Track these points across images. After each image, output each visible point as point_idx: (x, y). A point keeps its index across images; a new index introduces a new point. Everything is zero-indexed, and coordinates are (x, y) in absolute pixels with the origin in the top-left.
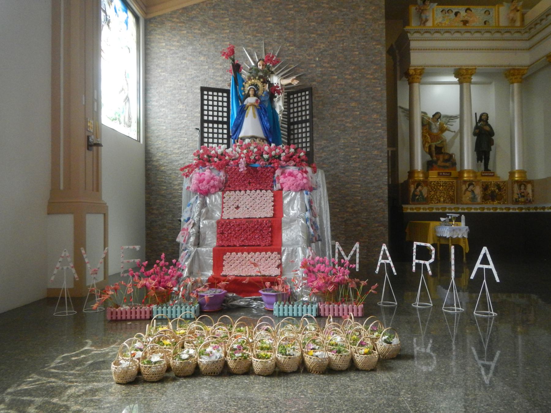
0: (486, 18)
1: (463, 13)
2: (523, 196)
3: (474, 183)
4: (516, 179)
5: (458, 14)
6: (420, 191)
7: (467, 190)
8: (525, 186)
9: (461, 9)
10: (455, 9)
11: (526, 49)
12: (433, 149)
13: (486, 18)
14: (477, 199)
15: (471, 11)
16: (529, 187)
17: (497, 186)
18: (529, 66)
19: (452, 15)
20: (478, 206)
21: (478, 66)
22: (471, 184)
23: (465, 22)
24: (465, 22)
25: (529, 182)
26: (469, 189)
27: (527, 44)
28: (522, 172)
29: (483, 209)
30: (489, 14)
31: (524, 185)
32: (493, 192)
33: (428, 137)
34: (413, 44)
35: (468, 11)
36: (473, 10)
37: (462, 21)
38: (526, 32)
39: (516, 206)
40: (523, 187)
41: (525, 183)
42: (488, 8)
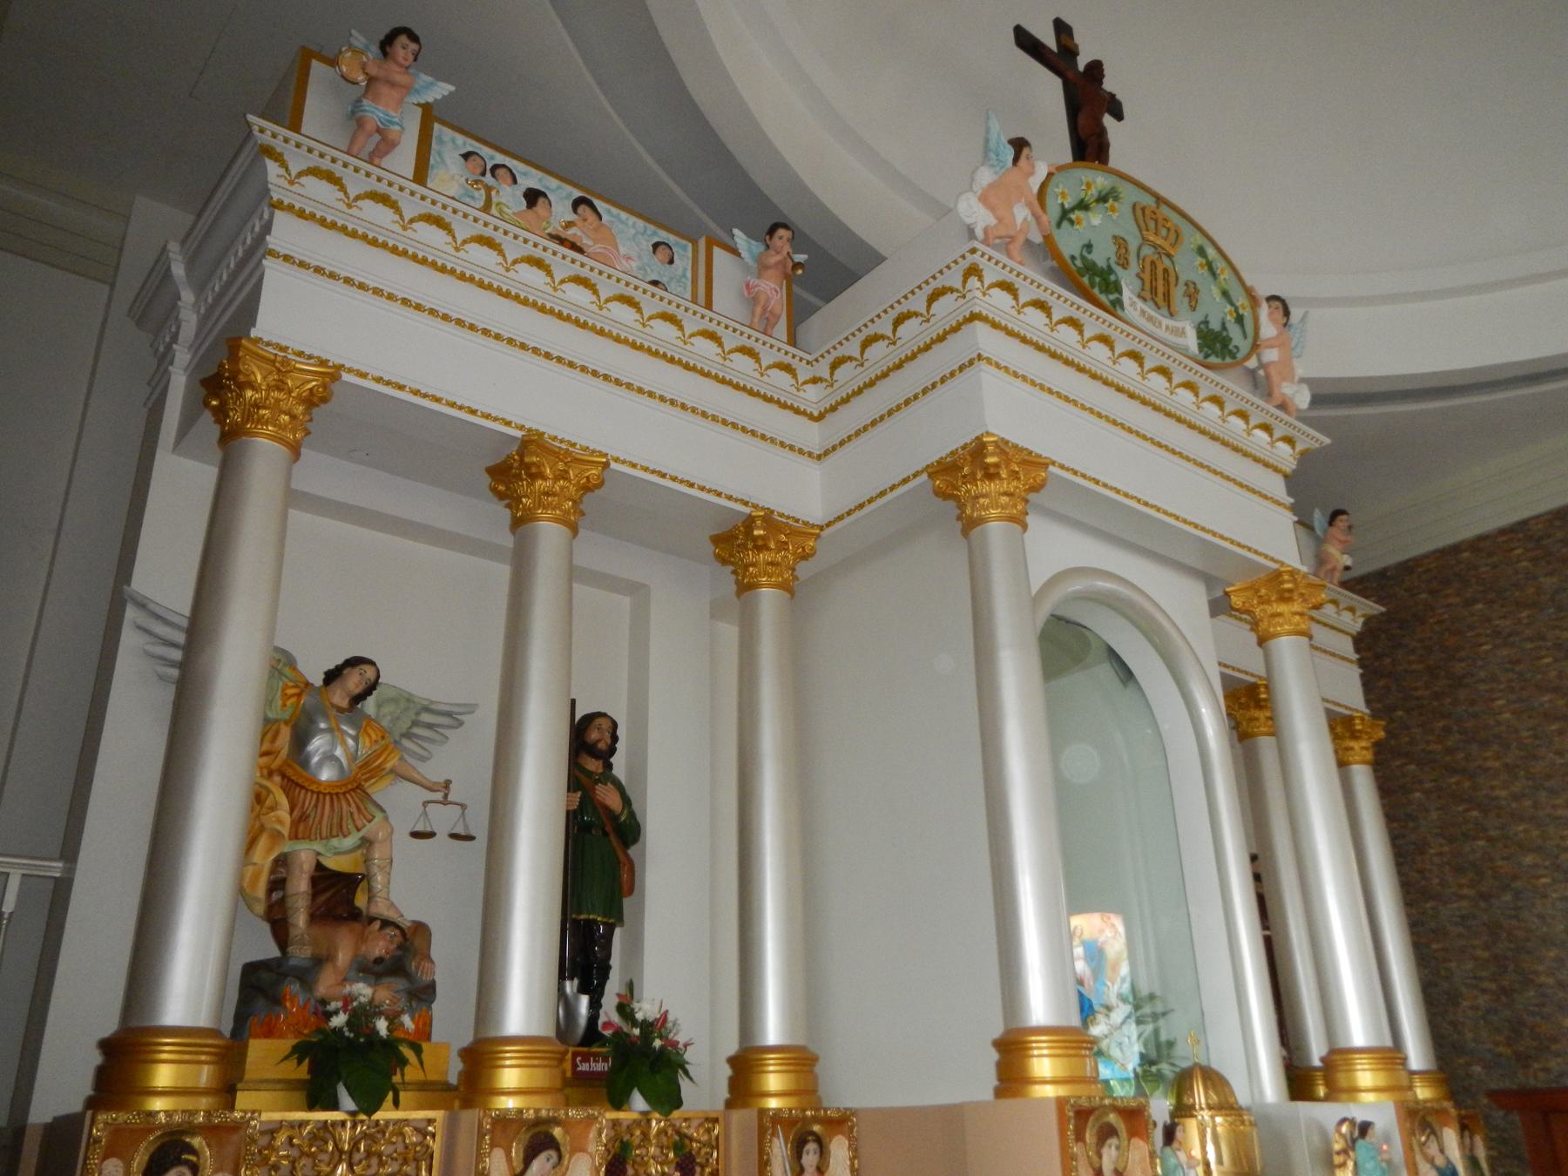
3: (557, 1132)
4: (773, 1103)
8: (823, 1151)
10: (525, 174)
11: (810, 454)
16: (839, 1149)
17: (677, 1147)
18: (822, 528)
19: (510, 197)
21: (617, 460)
25: (841, 1122)
27: (812, 436)
28: (801, 1060)
30: (671, 262)
31: (819, 1140)
34: (286, 233)
35: (582, 208)
36: (605, 218)
38: (815, 380)
40: (810, 1158)
41: (816, 1128)
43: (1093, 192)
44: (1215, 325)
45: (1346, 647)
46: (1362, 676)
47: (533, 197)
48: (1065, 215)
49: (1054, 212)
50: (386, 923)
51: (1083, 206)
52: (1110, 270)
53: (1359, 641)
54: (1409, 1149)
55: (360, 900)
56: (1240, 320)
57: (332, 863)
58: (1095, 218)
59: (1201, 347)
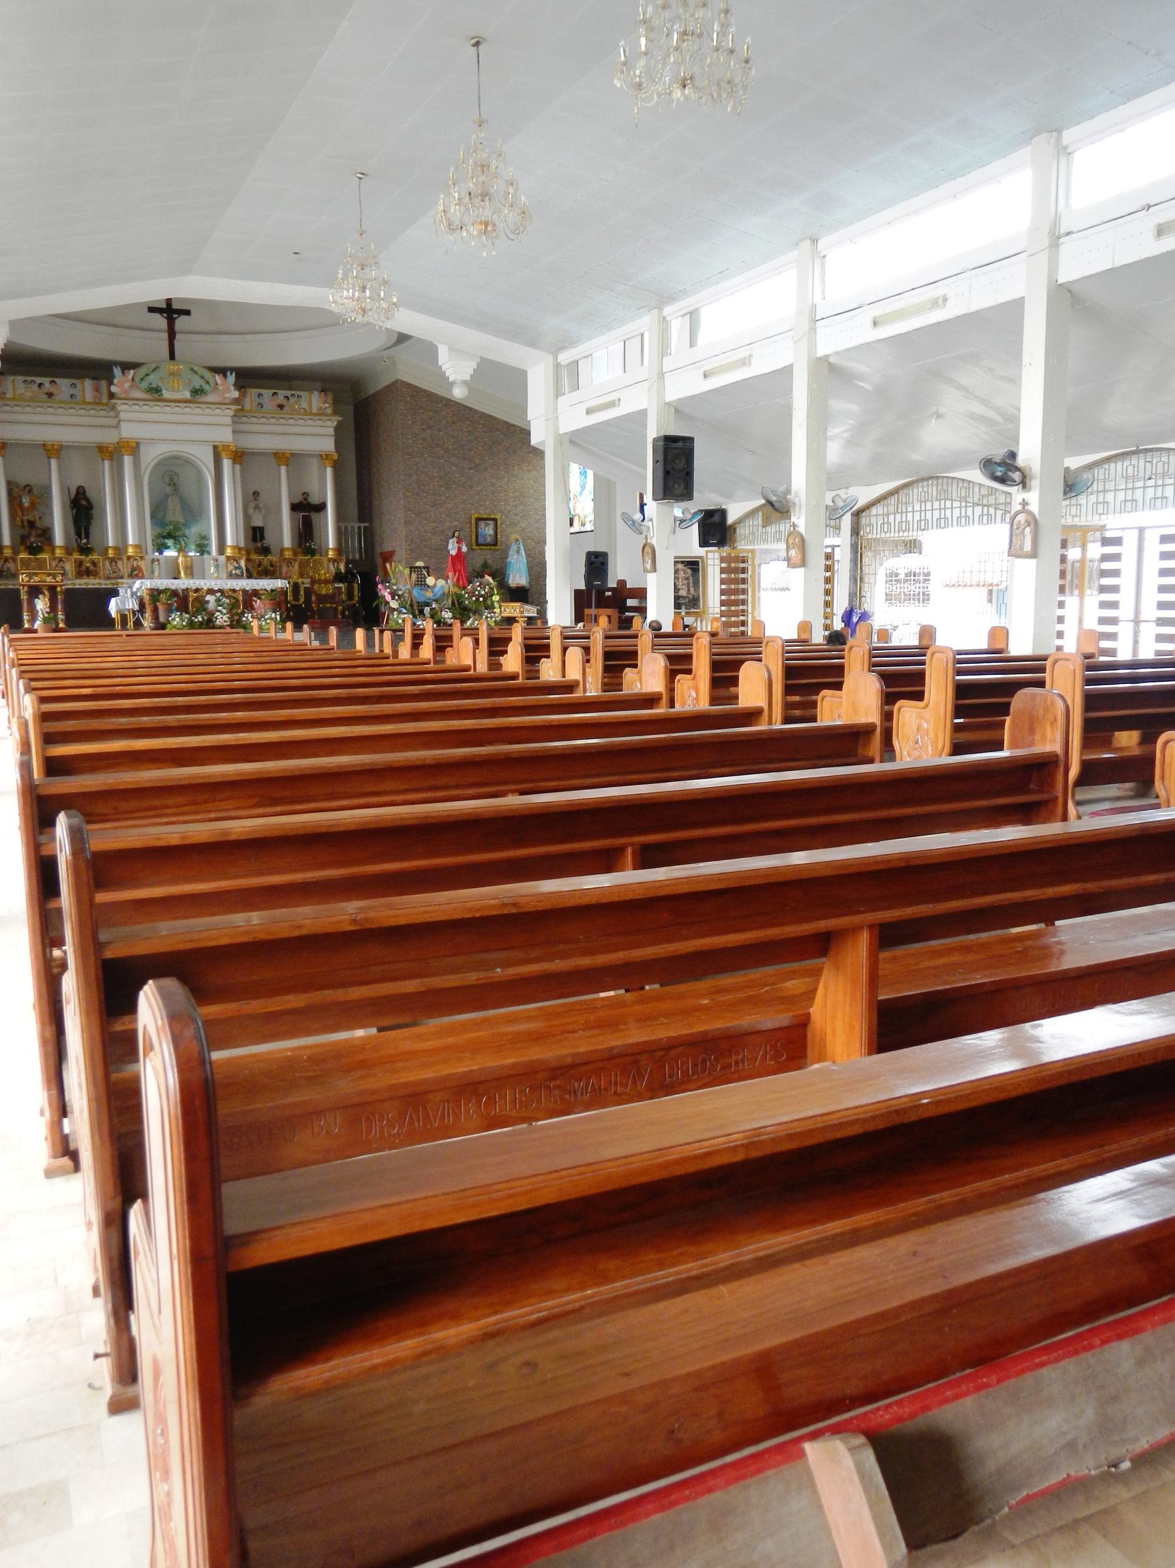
0: (72, 391)
1: (47, 385)
2: (115, 572)
5: (42, 386)
6: (8, 568)
7: (57, 566)
9: (46, 381)
12: (26, 524)
13: (72, 391)
14: (67, 574)
15: (55, 382)
19: (35, 387)
20: (70, 582)
22: (61, 560)
23: (50, 395)
24: (50, 395)
26: (60, 565)
28: (116, 549)
29: (74, 584)
32: (88, 568)
33: (19, 510)
37: (47, 393)
39: (108, 582)
40: (113, 564)
42: (74, 381)
43: (151, 369)
44: (197, 387)
45: (331, 431)
46: (335, 440)
47: (40, 385)
48: (142, 379)
49: (137, 379)
50: (40, 529)
51: (147, 375)
52: (158, 387)
53: (337, 429)
54: (227, 563)
55: (36, 525)
56: (208, 382)
57: (32, 519)
58: (152, 377)
59: (191, 396)
